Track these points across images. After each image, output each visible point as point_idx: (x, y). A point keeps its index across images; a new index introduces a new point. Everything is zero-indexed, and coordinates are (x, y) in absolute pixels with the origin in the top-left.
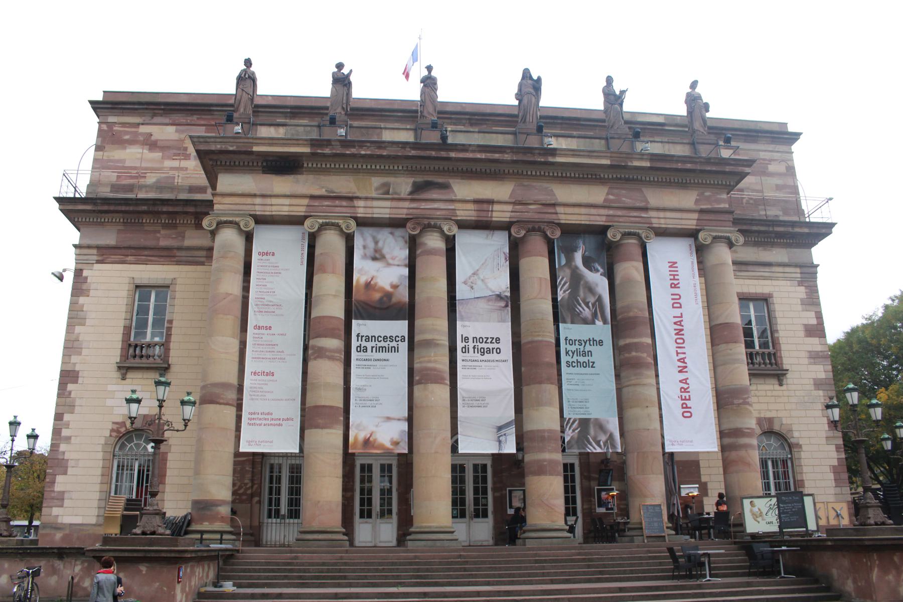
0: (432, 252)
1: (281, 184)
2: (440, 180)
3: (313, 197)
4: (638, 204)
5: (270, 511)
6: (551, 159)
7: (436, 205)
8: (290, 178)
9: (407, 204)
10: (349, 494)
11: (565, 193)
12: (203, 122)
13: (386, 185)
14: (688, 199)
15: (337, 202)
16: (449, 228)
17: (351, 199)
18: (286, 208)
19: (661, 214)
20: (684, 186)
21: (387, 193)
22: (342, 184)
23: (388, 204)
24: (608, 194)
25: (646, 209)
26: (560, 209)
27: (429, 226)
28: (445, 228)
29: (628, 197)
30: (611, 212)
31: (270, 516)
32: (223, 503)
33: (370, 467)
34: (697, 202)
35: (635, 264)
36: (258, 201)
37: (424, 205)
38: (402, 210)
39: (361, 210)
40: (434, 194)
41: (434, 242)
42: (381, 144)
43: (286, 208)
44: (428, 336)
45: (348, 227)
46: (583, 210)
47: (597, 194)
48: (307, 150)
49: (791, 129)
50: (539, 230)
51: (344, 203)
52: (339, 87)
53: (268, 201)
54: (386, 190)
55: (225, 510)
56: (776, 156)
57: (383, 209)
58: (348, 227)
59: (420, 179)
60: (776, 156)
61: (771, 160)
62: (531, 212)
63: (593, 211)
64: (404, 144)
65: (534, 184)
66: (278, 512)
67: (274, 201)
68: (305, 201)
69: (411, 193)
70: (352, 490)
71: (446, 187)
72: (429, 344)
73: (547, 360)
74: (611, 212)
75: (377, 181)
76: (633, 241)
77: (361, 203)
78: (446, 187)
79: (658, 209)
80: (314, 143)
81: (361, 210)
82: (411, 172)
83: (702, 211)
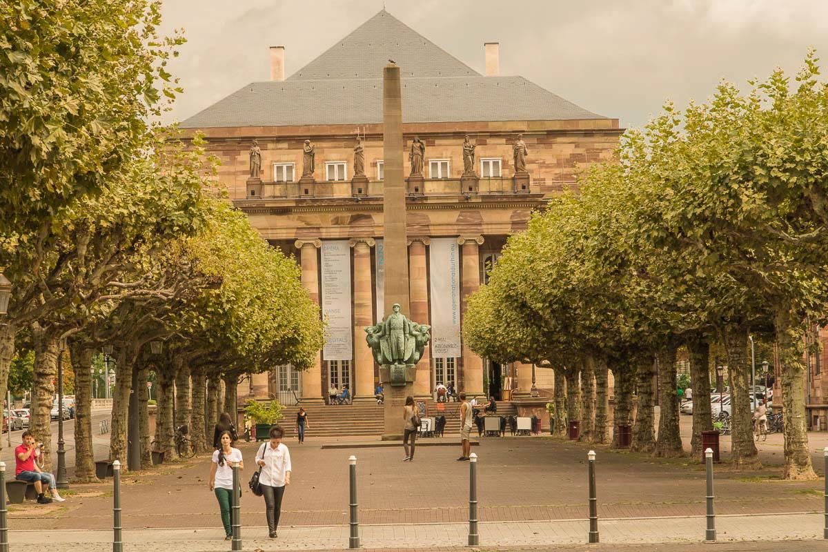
0: (360, 256)
1: (281, 221)
2: (366, 214)
3: (298, 228)
4: (476, 221)
5: (281, 387)
6: (425, 202)
7: (363, 229)
8: (285, 217)
9: (348, 230)
10: (325, 376)
11: (435, 217)
12: (220, 148)
13: (337, 218)
14: (506, 216)
15: (311, 230)
16: (371, 243)
17: (319, 228)
18: (284, 235)
19: (490, 227)
20: (504, 208)
21: (337, 223)
22: (314, 218)
23: (338, 230)
24: (459, 216)
25: (480, 224)
26: (431, 228)
27: (360, 242)
28: (368, 243)
29: (471, 217)
30: (460, 227)
31: (281, 389)
32: (265, 386)
33: (336, 362)
34: (512, 217)
35: (473, 257)
36: (270, 231)
37: (357, 230)
38: (346, 231)
39: (324, 234)
40: (363, 222)
41: (363, 250)
42: (332, 200)
43: (284, 235)
44: (361, 302)
45: (317, 244)
46: (444, 227)
47: (453, 216)
48: (294, 205)
49: (620, 128)
50: (419, 241)
51: (315, 231)
52: (307, 157)
53: (275, 231)
54: (337, 222)
55: (266, 390)
56: (606, 145)
57: (335, 232)
58: (317, 244)
59: (354, 213)
60: (606, 145)
61: (601, 150)
62: (415, 230)
63: (450, 227)
64: (345, 199)
65: (418, 212)
66: (286, 387)
67: (278, 231)
68: (295, 231)
69: (350, 223)
70: (327, 374)
71: (369, 217)
72: (360, 306)
73: (421, 312)
74: (460, 227)
75: (331, 216)
76: (473, 243)
77: (324, 230)
78: (369, 217)
79: (487, 224)
80: (297, 201)
81: (324, 234)
82: (349, 210)
83: (513, 223)
